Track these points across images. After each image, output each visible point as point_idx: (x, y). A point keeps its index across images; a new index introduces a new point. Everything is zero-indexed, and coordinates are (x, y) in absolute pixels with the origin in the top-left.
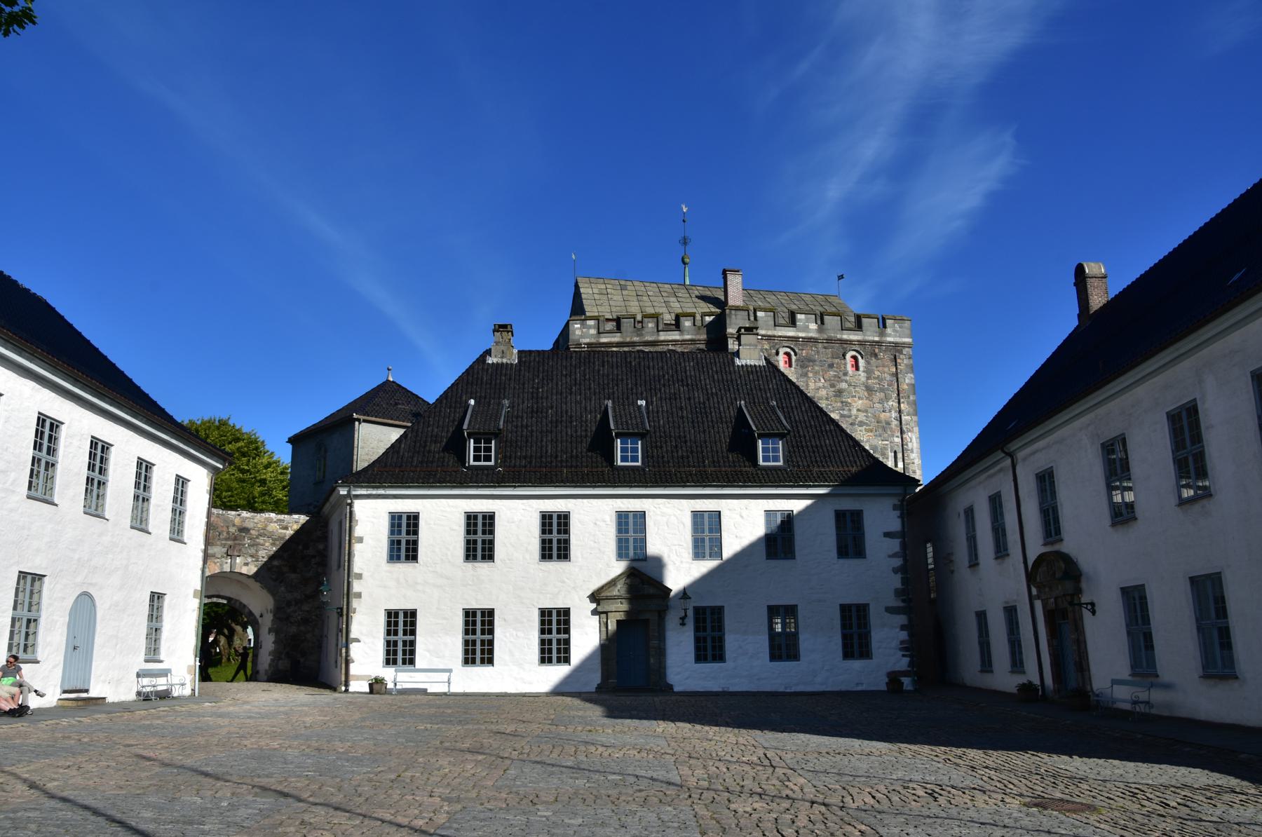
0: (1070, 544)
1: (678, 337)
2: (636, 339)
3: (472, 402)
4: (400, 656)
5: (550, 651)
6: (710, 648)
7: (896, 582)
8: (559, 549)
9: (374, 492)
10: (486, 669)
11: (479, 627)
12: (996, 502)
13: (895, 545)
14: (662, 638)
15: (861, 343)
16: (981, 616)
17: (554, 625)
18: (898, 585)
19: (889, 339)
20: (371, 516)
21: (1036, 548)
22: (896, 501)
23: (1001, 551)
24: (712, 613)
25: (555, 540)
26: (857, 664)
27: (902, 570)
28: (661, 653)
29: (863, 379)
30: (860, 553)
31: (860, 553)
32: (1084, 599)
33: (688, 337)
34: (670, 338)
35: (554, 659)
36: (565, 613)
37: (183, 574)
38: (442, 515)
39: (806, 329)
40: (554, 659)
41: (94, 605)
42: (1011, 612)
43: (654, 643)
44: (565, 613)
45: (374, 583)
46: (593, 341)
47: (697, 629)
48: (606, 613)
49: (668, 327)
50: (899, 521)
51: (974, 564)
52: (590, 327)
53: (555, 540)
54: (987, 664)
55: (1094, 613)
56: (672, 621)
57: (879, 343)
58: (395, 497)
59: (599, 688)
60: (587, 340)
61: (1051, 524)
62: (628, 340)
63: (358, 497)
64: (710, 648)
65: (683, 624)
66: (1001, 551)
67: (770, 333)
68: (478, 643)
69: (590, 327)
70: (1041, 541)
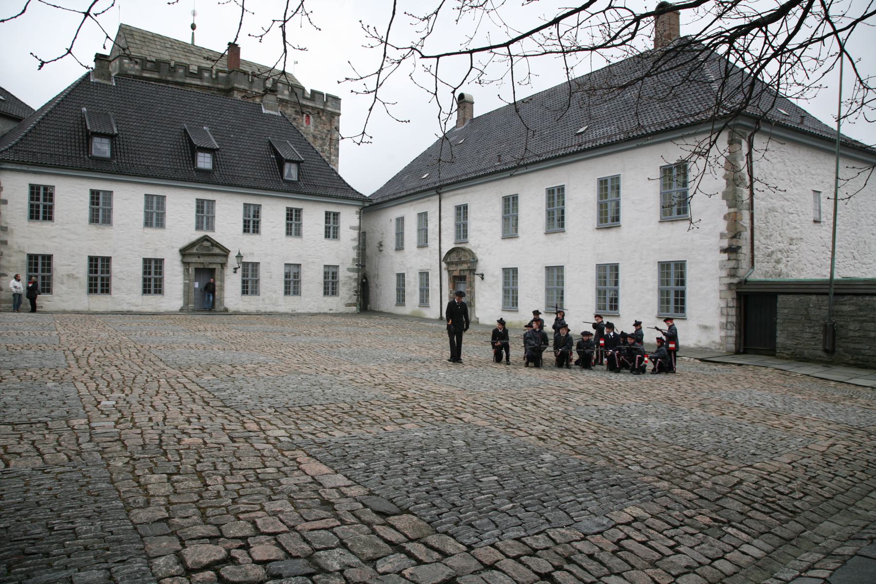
0: (473, 242)
1: (199, 83)
2: (170, 79)
3: (85, 109)
5: (96, 285)
6: (250, 286)
7: (353, 254)
9: (18, 168)
10: (158, 297)
11: (40, 267)
12: (423, 217)
13: (355, 234)
14: (222, 281)
15: (313, 108)
16: (401, 277)
18: (355, 257)
19: (329, 109)
21: (449, 244)
22: (357, 209)
23: (423, 243)
25: (154, 216)
27: (358, 248)
29: (312, 131)
30: (336, 236)
31: (336, 236)
32: (478, 271)
33: (206, 84)
34: (194, 82)
35: (152, 291)
36: (159, 262)
39: (283, 94)
40: (152, 291)
42: (424, 275)
44: (159, 262)
46: (138, 74)
47: (243, 276)
48: (189, 263)
49: (192, 75)
50: (358, 221)
51: (400, 247)
53: (154, 216)
54: (401, 300)
55: (483, 279)
56: (229, 271)
57: (323, 110)
59: (181, 310)
60: (133, 73)
61: (462, 231)
62: (164, 78)
64: (250, 286)
65: (235, 272)
66: (423, 243)
68: (153, 280)
70: (453, 241)
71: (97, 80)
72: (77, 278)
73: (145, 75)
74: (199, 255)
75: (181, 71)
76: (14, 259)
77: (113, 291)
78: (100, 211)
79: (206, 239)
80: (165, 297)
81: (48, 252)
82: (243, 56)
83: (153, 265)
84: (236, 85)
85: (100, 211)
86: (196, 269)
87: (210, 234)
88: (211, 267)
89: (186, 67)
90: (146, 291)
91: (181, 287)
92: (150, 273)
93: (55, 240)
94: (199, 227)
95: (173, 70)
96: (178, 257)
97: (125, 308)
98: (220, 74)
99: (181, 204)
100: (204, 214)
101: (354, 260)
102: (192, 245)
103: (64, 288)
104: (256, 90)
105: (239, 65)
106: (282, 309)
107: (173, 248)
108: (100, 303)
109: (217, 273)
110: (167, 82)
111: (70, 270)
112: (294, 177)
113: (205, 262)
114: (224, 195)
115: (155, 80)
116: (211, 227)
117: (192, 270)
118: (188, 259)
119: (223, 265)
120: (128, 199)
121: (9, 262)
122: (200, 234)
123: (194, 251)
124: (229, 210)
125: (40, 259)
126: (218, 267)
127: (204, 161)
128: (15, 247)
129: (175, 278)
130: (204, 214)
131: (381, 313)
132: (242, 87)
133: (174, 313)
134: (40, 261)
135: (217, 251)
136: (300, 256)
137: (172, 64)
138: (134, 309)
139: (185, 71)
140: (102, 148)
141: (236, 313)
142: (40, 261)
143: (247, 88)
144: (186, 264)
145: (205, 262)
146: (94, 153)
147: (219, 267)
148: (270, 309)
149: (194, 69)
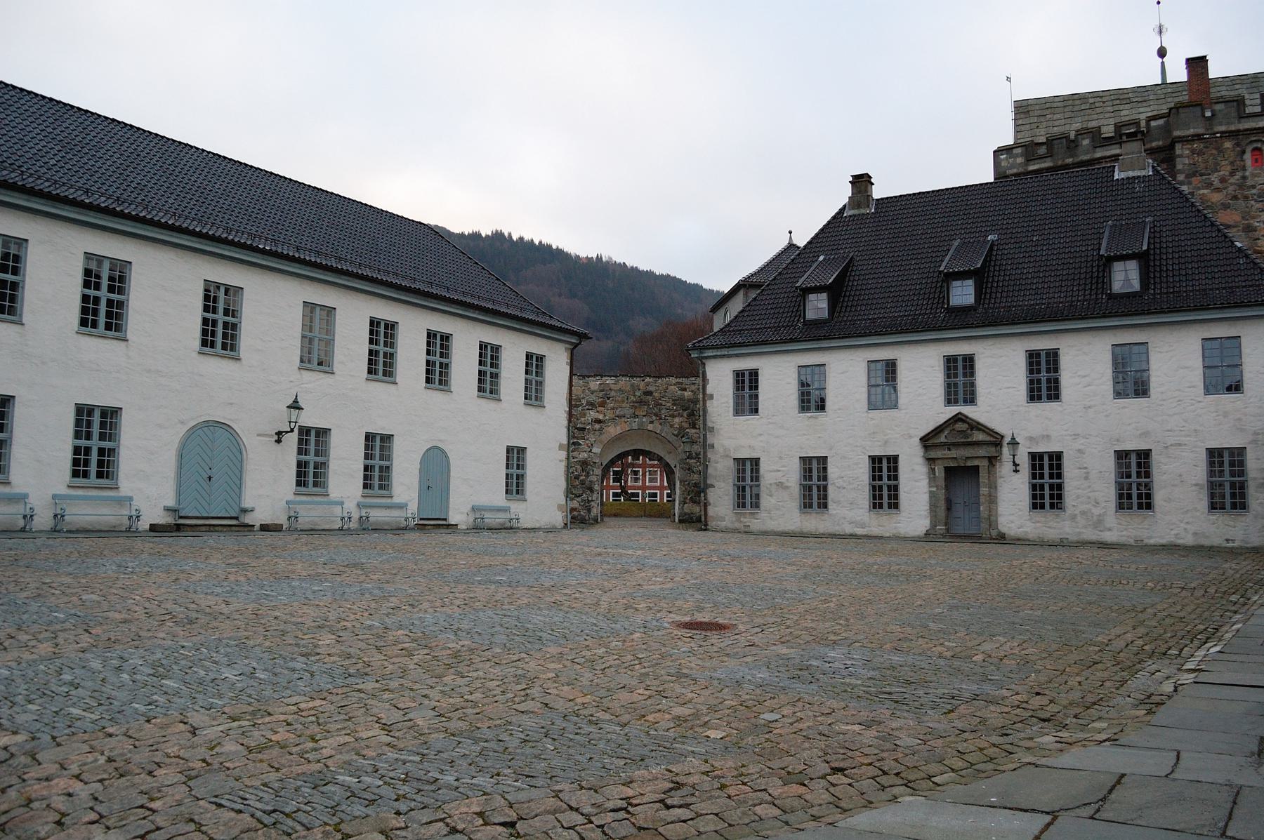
2: (1069, 161)
4: (885, 501)
8: (1049, 389)
14: (993, 486)
17: (884, 472)
20: (720, 376)
24: (1051, 458)
26: (1219, 518)
28: (993, 500)
36: (893, 460)
37: (545, 433)
38: (778, 374)
41: (447, 457)
43: (984, 490)
44: (893, 460)
45: (731, 434)
46: (1021, 170)
49: (1108, 141)
52: (1017, 156)
56: (1005, 468)
58: (737, 356)
59: (927, 534)
60: (1015, 171)
62: (1060, 163)
63: (707, 358)
67: (1233, 128)
69: (1017, 156)
71: (1123, 175)
72: (787, 487)
73: (1031, 168)
74: (950, 446)
75: (1086, 142)
76: (719, 466)
77: (831, 505)
78: (1132, 381)
79: (959, 418)
80: (903, 514)
81: (755, 456)
82: (1214, 71)
83: (885, 465)
84: (1177, 133)
85: (1132, 381)
86: (947, 470)
87: (967, 410)
88: (970, 464)
89: (1095, 134)
90: (876, 504)
91: (926, 497)
92: (880, 478)
93: (761, 438)
94: (950, 401)
95: (1072, 144)
96: (918, 451)
97: (849, 529)
98: (1153, 123)
99: (921, 367)
100: (960, 376)
101: (561, 447)
102: (938, 430)
103: (773, 501)
104: (1223, 128)
105: (1207, 92)
106: (1109, 537)
107: (911, 437)
108: (814, 522)
109: (983, 474)
110: (1066, 167)
111: (781, 473)
112: (1117, 286)
113: (962, 455)
114: (990, 342)
115: (1048, 170)
116: (971, 399)
117: (939, 471)
118: (933, 454)
119: (993, 460)
120: (846, 371)
121: (716, 469)
122: (953, 410)
123: (942, 439)
124: (1001, 365)
125: (1046, 458)
126: (983, 464)
127: (962, 293)
128: (721, 450)
129: (916, 484)
130: (960, 376)
131: (1002, 538)
132: (1192, 131)
133: (915, 540)
134: (1046, 462)
135: (980, 437)
136: (1146, 434)
137: (1072, 137)
138: (859, 531)
139: (1093, 140)
140: (1125, 277)
141: (1019, 541)
142: (1046, 462)
143: (1200, 131)
144: (930, 461)
145: (962, 455)
146: (825, 315)
147: (985, 463)
148: (1090, 535)
149: (1108, 131)
